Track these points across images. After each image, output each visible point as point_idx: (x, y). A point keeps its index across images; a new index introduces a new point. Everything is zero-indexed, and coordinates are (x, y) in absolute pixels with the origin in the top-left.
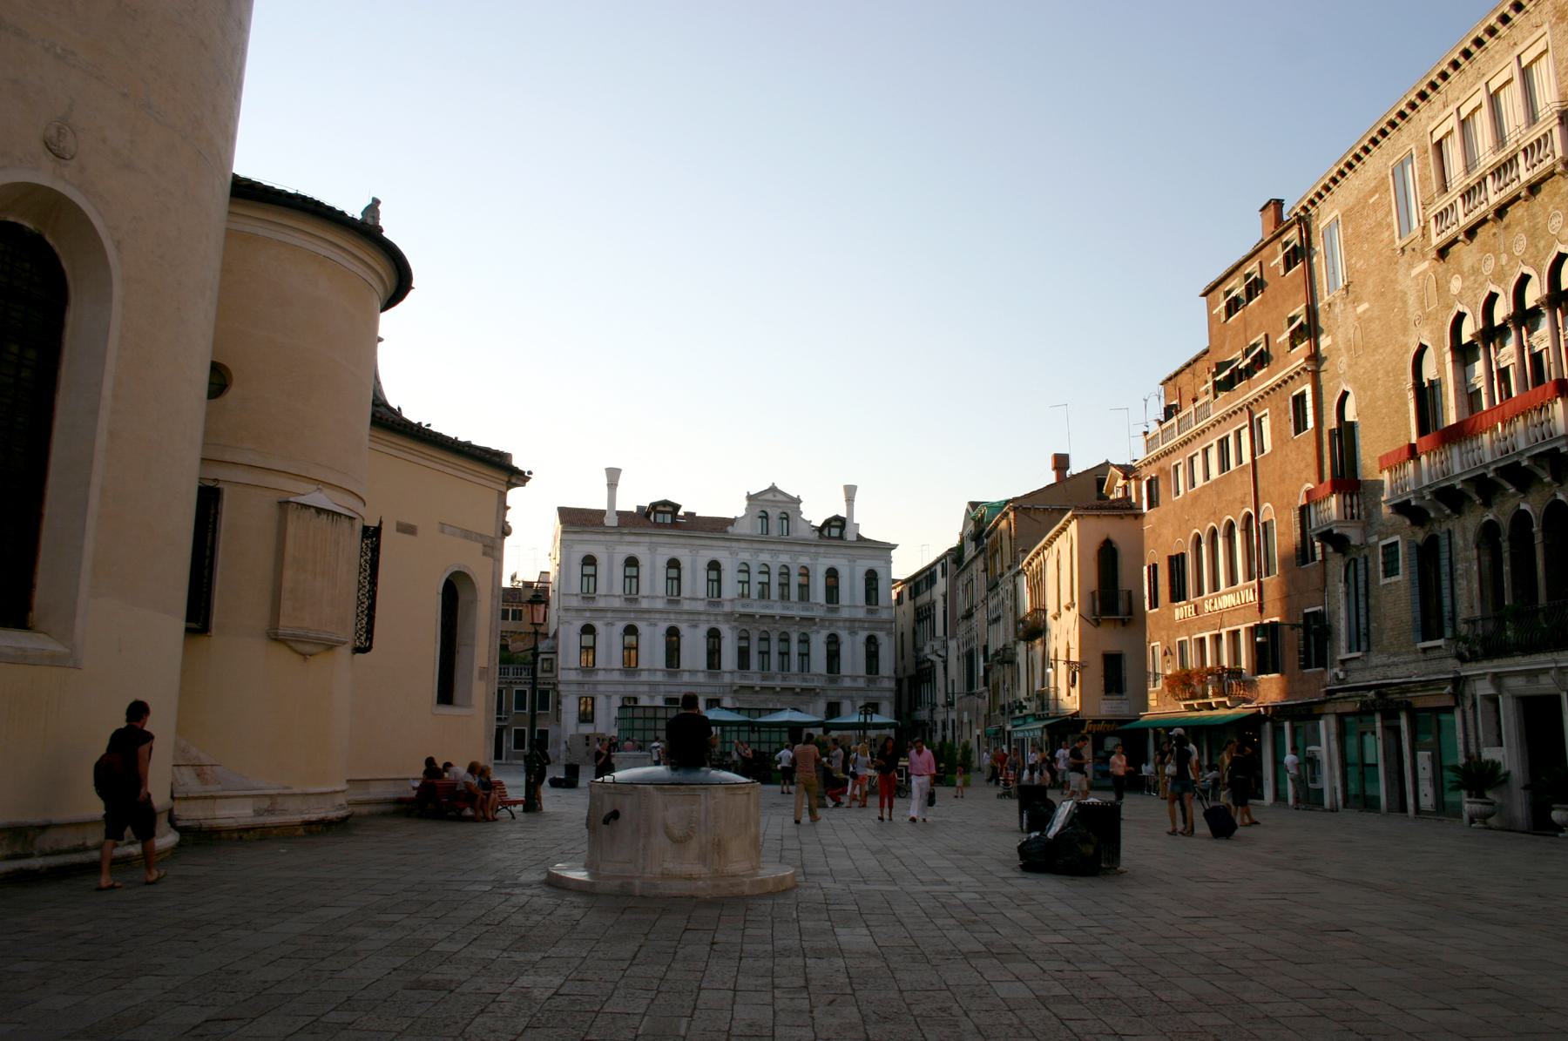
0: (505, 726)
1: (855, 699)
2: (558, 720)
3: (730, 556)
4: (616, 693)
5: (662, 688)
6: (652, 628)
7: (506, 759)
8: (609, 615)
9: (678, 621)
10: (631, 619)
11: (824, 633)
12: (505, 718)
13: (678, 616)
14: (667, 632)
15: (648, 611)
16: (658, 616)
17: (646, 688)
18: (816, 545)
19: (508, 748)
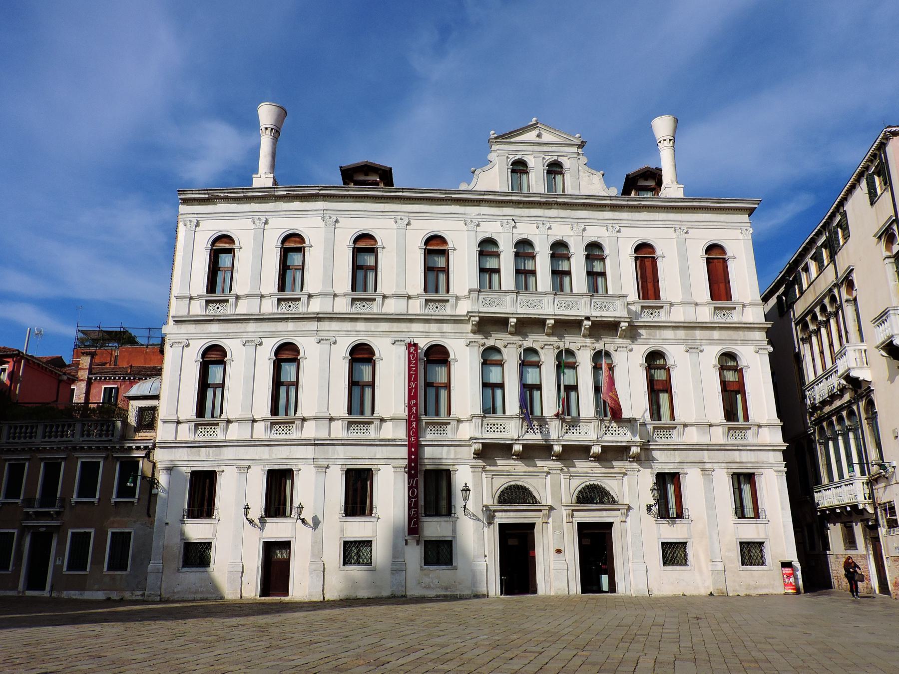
0: (57, 528)
1: (708, 466)
2: (149, 516)
3: (465, 228)
4: (258, 461)
5: (341, 452)
6: (325, 346)
7: (51, 591)
8: (251, 327)
9: (373, 334)
10: (287, 332)
11: (640, 351)
12: (58, 513)
13: (372, 326)
14: (351, 354)
15: (318, 318)
16: (335, 326)
17: (309, 451)
18: (614, 208)
19: (58, 568)
